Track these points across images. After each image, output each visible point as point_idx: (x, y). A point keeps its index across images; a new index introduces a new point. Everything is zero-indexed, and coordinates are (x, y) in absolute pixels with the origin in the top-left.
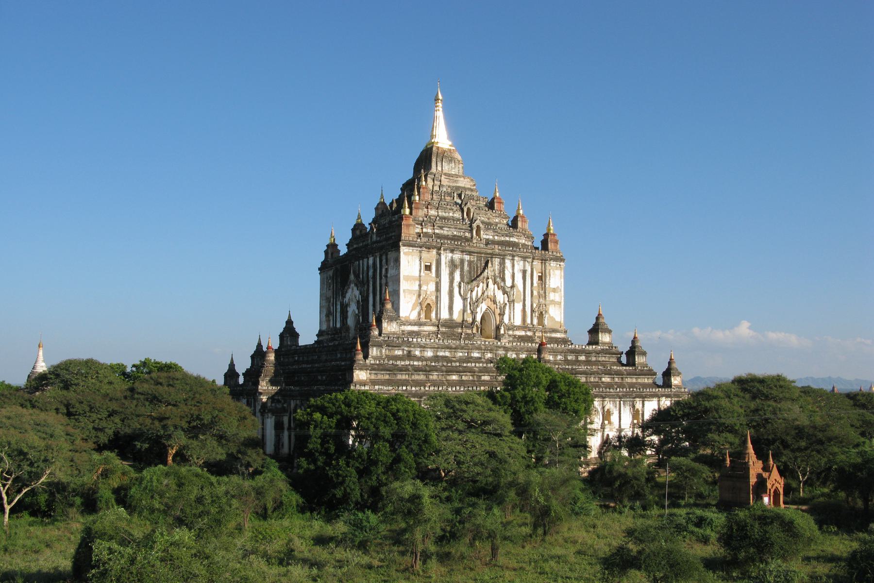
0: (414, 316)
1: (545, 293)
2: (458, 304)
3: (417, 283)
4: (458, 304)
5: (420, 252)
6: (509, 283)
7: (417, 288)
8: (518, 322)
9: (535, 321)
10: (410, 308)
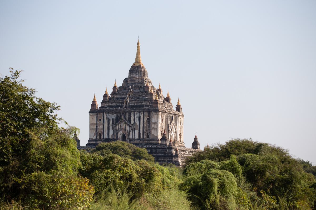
0: (95, 138)
1: (150, 125)
2: (111, 132)
3: (96, 126)
4: (111, 132)
5: (97, 114)
6: (132, 122)
7: (95, 128)
8: (137, 137)
9: (145, 137)
10: (93, 136)
